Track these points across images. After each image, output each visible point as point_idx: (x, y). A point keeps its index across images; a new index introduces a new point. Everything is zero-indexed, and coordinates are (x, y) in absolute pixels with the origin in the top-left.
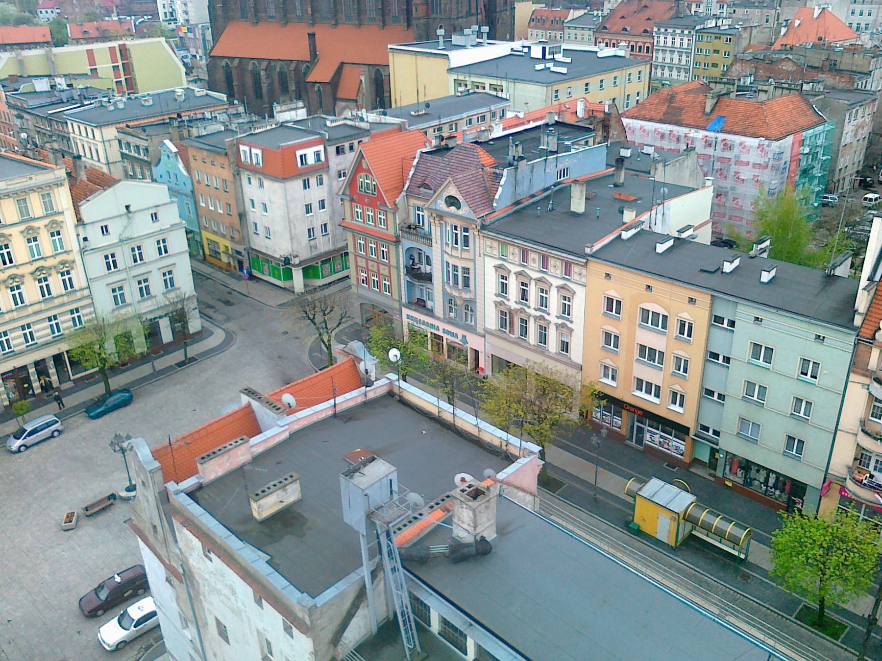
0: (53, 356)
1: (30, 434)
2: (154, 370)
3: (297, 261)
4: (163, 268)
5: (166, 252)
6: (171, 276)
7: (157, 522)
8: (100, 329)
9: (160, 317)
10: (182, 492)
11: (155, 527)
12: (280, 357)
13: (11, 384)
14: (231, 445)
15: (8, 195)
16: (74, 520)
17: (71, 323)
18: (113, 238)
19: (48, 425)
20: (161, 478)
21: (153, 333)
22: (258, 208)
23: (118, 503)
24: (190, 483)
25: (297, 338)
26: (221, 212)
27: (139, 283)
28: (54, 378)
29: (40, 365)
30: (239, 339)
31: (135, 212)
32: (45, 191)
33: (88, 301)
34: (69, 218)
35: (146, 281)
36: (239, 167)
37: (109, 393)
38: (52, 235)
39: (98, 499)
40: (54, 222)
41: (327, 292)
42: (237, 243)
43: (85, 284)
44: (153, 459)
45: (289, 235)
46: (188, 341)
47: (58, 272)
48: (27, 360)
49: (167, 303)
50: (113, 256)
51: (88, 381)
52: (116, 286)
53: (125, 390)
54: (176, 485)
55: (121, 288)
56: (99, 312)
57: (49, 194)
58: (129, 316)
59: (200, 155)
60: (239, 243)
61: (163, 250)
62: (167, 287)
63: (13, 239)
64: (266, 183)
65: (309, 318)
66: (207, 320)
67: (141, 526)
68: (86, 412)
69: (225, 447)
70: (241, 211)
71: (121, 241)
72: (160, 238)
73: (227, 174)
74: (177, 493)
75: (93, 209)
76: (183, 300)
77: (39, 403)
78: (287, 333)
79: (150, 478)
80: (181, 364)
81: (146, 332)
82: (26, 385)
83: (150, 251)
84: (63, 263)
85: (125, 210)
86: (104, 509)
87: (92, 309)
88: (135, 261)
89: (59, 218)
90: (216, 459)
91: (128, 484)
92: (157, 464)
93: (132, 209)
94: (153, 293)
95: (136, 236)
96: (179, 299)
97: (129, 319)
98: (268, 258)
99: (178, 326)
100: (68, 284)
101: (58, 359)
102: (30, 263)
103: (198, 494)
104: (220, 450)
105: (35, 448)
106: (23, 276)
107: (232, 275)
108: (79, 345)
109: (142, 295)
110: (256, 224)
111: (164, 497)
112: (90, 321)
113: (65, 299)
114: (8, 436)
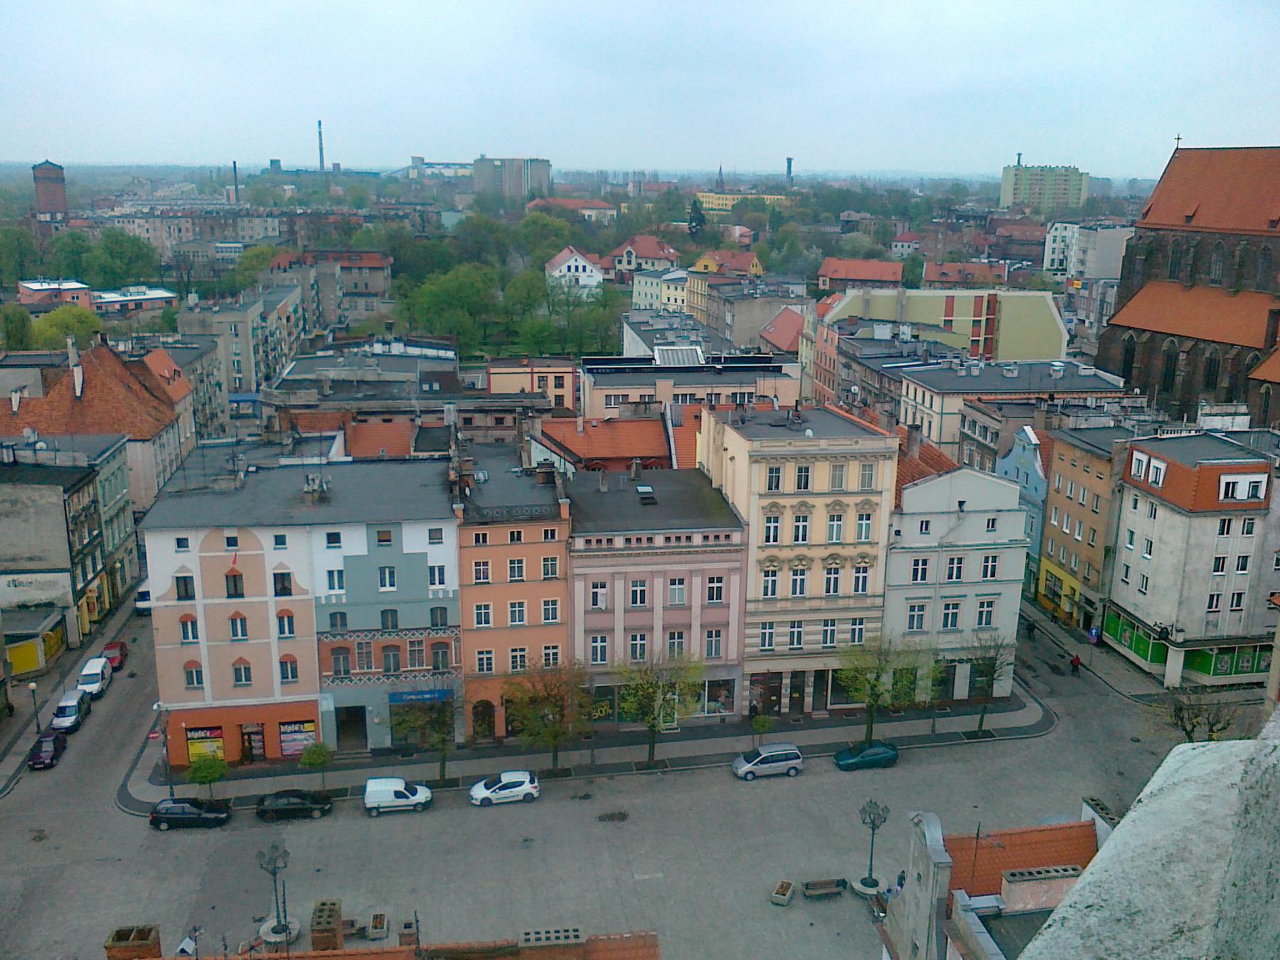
0: (816, 671)
1: (765, 761)
2: (933, 731)
3: (1180, 638)
4: (982, 595)
5: (993, 575)
6: (990, 609)
7: (921, 942)
8: (882, 654)
9: (961, 661)
10: (972, 910)
11: (915, 947)
12: (1121, 774)
13: (758, 690)
14: (1057, 871)
15: (825, 457)
16: (788, 894)
17: (849, 636)
18: (931, 540)
19: (787, 758)
20: (947, 880)
21: (945, 680)
22: (1139, 546)
23: (847, 894)
24: (986, 902)
25: (1153, 753)
26: (1079, 538)
27: (947, 607)
28: (809, 700)
29: (798, 676)
30: (1062, 726)
31: (968, 512)
32: (869, 461)
33: (877, 614)
34: (887, 502)
35: (956, 606)
36: (1126, 480)
37: (870, 743)
38: (861, 518)
39: (823, 879)
40: (868, 502)
41: (1226, 696)
42: (1092, 588)
43: (880, 591)
44: (943, 848)
45: (1177, 596)
46: (989, 706)
47: (853, 567)
48: (786, 666)
49: (976, 644)
50: (925, 562)
51: (846, 718)
52: (917, 603)
53: (891, 744)
54: (967, 898)
55: (922, 608)
56: (887, 631)
57: (871, 466)
58: (924, 648)
59: (1070, 454)
60: (1096, 589)
61: (990, 570)
62: (980, 623)
63: (815, 511)
64: (1161, 512)
65: (1184, 729)
66: (1020, 685)
67: (893, 937)
68: (835, 757)
69: (1048, 872)
70: (1111, 544)
71: (941, 546)
72: (991, 553)
73: (1103, 488)
74: (967, 909)
75: (917, 497)
76: (998, 647)
77: (784, 725)
78: (1138, 741)
79: (932, 874)
80: (971, 735)
81: (939, 676)
82: (774, 698)
83: (973, 567)
84: (863, 556)
85: (956, 507)
86: (827, 897)
87: (879, 625)
88: (950, 577)
89: (875, 499)
90: (1031, 883)
91: (867, 875)
92: (947, 858)
93: (965, 507)
94: (960, 625)
95: (960, 543)
96: (993, 644)
97: (924, 651)
98: (1134, 622)
99: (982, 681)
100: (860, 584)
101: (820, 675)
102: (825, 546)
103: (992, 923)
104: (1039, 873)
105: (764, 782)
106: (812, 560)
107: (1071, 633)
108: (852, 666)
109: (945, 625)
110: (1128, 567)
111: (945, 910)
112: (874, 639)
113: (852, 603)
114: (736, 755)
